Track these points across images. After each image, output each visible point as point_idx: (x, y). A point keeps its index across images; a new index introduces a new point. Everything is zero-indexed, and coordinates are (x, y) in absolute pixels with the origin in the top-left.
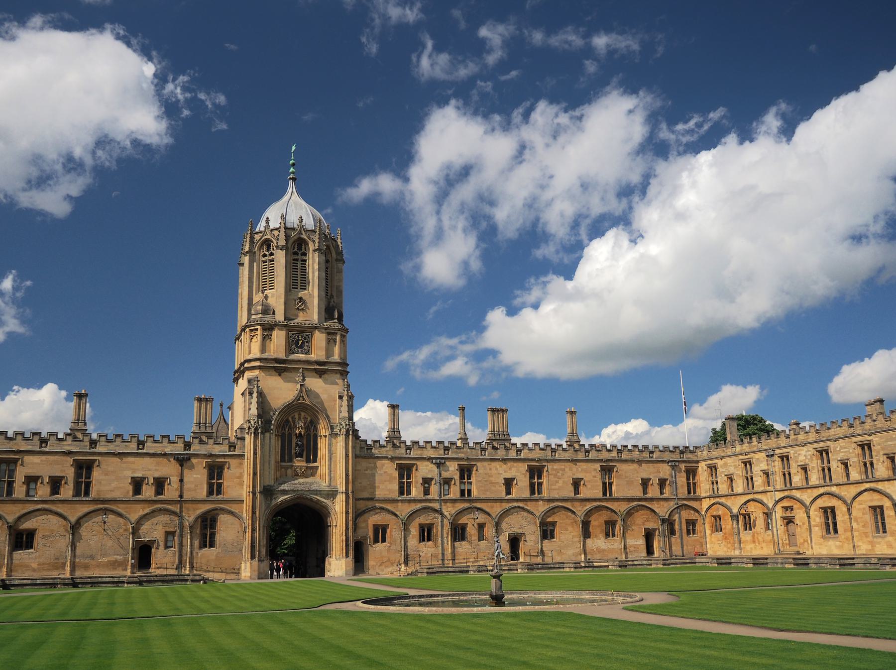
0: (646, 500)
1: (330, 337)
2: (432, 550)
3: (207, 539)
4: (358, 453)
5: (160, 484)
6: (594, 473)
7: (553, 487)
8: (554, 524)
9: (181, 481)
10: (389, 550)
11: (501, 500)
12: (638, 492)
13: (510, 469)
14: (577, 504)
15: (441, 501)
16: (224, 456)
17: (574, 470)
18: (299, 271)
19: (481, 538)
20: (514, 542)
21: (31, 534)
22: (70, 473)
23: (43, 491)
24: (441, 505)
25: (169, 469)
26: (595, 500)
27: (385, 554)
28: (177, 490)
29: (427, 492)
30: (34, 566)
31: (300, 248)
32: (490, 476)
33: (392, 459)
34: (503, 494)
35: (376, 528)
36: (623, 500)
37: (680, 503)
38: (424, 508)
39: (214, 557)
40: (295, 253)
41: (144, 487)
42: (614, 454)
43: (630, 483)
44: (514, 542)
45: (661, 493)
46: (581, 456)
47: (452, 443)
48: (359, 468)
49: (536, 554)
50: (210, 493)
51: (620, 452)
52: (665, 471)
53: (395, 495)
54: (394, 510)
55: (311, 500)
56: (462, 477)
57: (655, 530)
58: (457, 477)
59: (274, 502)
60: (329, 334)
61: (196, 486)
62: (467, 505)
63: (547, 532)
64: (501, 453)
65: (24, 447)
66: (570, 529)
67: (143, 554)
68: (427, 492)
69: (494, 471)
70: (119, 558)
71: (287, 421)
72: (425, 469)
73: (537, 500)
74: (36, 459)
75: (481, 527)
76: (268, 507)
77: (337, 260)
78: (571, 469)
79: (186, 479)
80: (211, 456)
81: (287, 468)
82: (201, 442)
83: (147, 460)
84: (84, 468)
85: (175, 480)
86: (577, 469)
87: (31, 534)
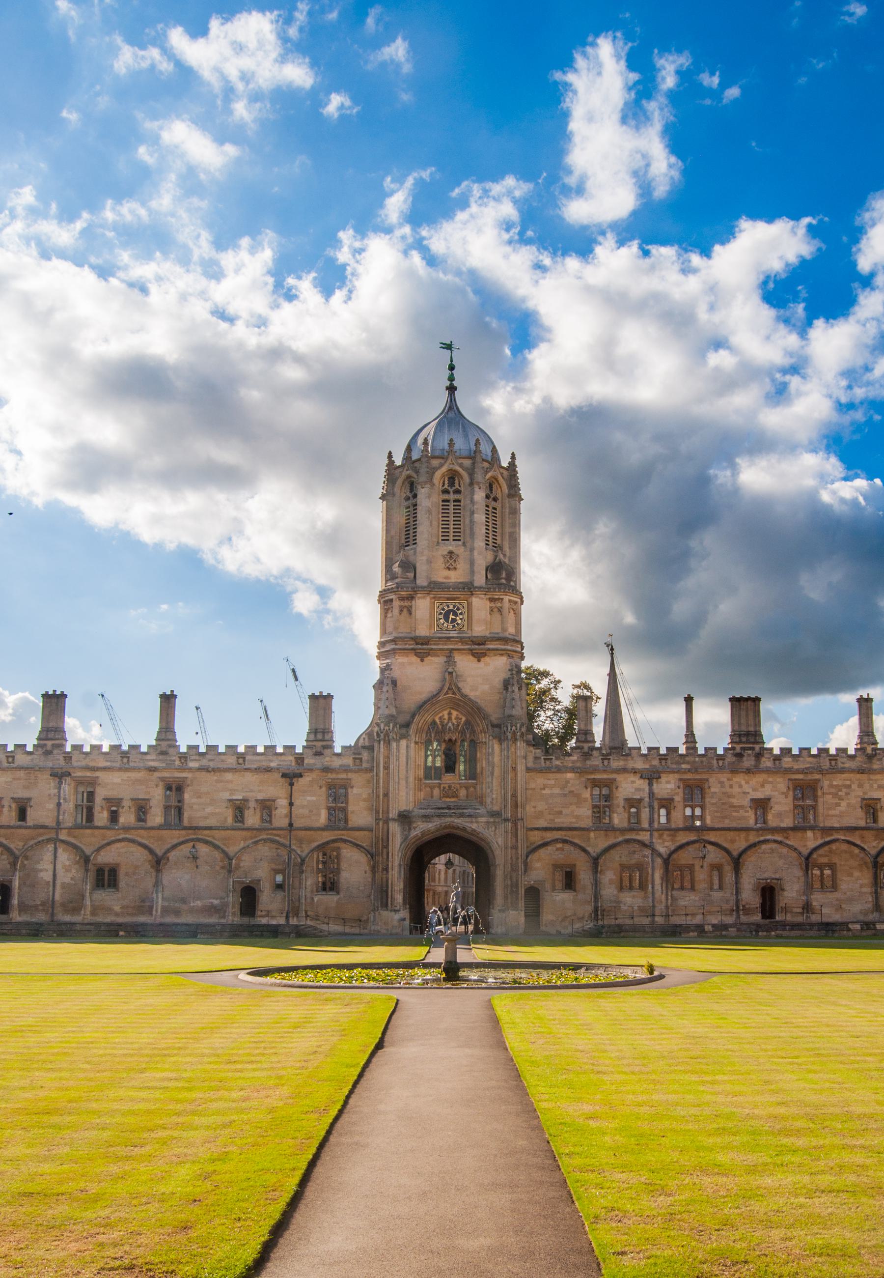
1: (493, 605)
4: (530, 765)
7: (832, 812)
9: (291, 804)
11: (747, 830)
13: (763, 786)
14: (869, 835)
17: (867, 786)
18: (451, 515)
20: (768, 894)
22: (157, 796)
24: (651, 835)
25: (276, 790)
28: (286, 816)
30: (117, 908)
32: (729, 797)
38: (627, 841)
39: (334, 905)
40: (446, 492)
41: (247, 813)
44: (768, 894)
47: (672, 750)
48: (532, 785)
49: (800, 910)
53: (587, 822)
54: (583, 845)
55: (464, 829)
59: (413, 833)
60: (492, 600)
61: (311, 811)
62: (692, 837)
64: (748, 762)
65: (102, 764)
66: (857, 874)
67: (249, 896)
69: (736, 790)
70: (216, 902)
71: (434, 722)
72: (630, 787)
73: (804, 829)
76: (405, 839)
77: (510, 496)
78: (860, 786)
79: (297, 802)
80: (326, 770)
81: (432, 788)
82: (318, 754)
84: (176, 788)
85: (283, 802)
86: (871, 786)
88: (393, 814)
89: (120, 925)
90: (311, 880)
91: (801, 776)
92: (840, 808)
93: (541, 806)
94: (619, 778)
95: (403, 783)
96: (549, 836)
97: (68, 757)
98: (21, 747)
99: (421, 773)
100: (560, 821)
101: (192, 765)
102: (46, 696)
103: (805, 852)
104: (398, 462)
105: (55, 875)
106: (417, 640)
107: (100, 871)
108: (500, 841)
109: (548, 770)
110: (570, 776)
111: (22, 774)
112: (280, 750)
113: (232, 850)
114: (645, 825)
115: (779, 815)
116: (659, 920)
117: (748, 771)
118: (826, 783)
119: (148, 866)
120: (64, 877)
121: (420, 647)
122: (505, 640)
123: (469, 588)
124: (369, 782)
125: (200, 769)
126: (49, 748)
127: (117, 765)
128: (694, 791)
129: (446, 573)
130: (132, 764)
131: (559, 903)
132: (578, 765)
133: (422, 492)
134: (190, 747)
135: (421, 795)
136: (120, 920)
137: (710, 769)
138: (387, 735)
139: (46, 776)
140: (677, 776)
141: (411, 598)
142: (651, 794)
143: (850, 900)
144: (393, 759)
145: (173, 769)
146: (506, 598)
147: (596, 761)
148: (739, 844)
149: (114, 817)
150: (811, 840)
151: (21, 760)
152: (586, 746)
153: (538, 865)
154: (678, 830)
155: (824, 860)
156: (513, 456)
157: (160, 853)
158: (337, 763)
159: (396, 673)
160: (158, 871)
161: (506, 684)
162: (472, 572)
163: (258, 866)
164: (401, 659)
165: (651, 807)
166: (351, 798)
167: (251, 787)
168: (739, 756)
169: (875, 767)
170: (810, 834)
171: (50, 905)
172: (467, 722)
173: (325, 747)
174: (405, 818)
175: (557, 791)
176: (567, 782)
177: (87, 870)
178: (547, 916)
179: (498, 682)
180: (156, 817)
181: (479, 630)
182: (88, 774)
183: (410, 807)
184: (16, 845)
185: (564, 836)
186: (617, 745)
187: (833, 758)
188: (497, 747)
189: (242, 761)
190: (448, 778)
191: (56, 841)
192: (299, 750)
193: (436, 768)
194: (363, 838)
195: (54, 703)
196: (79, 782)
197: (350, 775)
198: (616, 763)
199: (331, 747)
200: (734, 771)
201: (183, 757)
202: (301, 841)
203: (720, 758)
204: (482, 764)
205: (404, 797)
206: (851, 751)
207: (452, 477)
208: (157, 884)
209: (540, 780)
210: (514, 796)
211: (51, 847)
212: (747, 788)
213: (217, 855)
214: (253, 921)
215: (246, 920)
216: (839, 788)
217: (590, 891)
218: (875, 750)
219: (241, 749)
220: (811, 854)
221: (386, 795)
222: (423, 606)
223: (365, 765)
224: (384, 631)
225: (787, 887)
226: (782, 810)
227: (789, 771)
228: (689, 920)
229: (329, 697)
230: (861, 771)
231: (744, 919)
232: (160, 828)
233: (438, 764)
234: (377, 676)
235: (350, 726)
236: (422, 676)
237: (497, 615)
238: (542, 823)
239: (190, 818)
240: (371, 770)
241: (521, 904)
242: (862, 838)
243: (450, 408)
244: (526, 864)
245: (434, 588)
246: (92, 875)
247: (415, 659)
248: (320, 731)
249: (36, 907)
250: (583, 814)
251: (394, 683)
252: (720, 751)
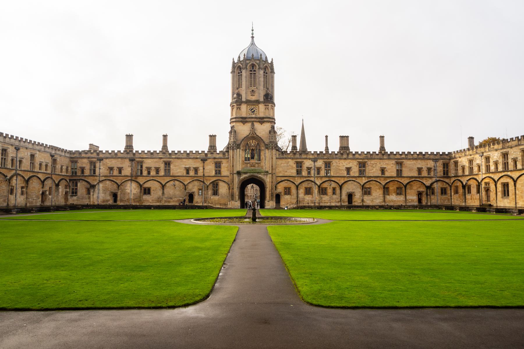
0: (419, 177)
2: (310, 199)
3: (215, 193)
4: (277, 157)
5: (196, 170)
6: (392, 165)
8: (370, 188)
9: (204, 169)
10: (291, 198)
11: (344, 177)
12: (416, 174)
14: (382, 179)
15: (314, 177)
16: (221, 158)
17: (382, 163)
19: (334, 193)
20: (350, 196)
21: (149, 189)
22: (162, 166)
23: (153, 173)
25: (198, 164)
26: (392, 177)
27: (289, 199)
29: (309, 173)
30: (151, 201)
31: (253, 68)
33: (292, 159)
34: (345, 175)
35: (285, 188)
36: (407, 177)
37: (438, 179)
38: (307, 180)
41: (190, 171)
42: (403, 156)
43: (411, 170)
44: (350, 196)
45: (429, 174)
46: (385, 157)
47: (321, 152)
48: (278, 163)
50: (216, 173)
51: (406, 155)
52: (431, 164)
56: (326, 167)
57: (423, 192)
58: (323, 167)
59: (241, 178)
60: (265, 105)
62: (327, 179)
63: (366, 191)
64: (345, 156)
66: (378, 191)
68: (309, 173)
69: (341, 164)
71: (248, 144)
72: (308, 163)
73: (362, 177)
74: (149, 161)
75: (334, 189)
76: (239, 179)
77: (271, 72)
78: (380, 163)
79: (205, 168)
80: (215, 158)
81: (247, 163)
82: (212, 153)
83: (191, 160)
84: (168, 164)
87: (149, 189)
88: (235, 172)
89: (152, 206)
90: (210, 192)
91: (361, 161)
92: (373, 169)
93: (281, 169)
94: (305, 161)
95: (238, 162)
96: (283, 179)
97: (134, 154)
98: (119, 151)
99: (244, 159)
100: (286, 174)
101: (173, 157)
102: (127, 135)
103: (362, 184)
104: (236, 62)
105: (131, 191)
106: (242, 118)
107: (145, 189)
108: (268, 180)
109: (283, 158)
110: (289, 160)
111: (120, 160)
112: (200, 152)
113: (186, 183)
114: (313, 175)
115: (354, 172)
116: (317, 204)
117: (345, 159)
118: (369, 163)
119: (160, 188)
120: (134, 191)
121: (243, 120)
122: (269, 118)
123: (257, 102)
124: (228, 162)
125: (175, 158)
126: (128, 151)
127: (149, 157)
128: (328, 165)
129: (251, 97)
130: (154, 157)
131: (285, 200)
132: (292, 157)
133: (244, 72)
134: (172, 151)
135: (244, 166)
136: (151, 204)
137: (333, 159)
138: (233, 147)
139: (128, 160)
140: (323, 160)
141: (240, 105)
142: (315, 166)
143: (376, 199)
144: (235, 155)
145: (167, 157)
146: (270, 105)
147: (297, 156)
148: (341, 181)
149: (149, 173)
150: (364, 180)
151: (119, 155)
152: (295, 151)
153: (280, 187)
154: (322, 177)
155: (368, 186)
156: (272, 60)
157: (164, 184)
158: (218, 156)
159: (235, 129)
160: (163, 189)
161: (270, 132)
162: (260, 97)
163: (194, 188)
164: (238, 124)
165: (315, 170)
166: (222, 167)
167: (191, 164)
168: (342, 154)
169: (385, 158)
170: (364, 178)
171: (128, 200)
172: (258, 144)
173: (215, 151)
174: (239, 173)
175: (285, 165)
176: (289, 162)
177: (141, 189)
178: (283, 203)
179: (267, 131)
180: (162, 173)
181: (261, 115)
182: (141, 160)
183: (240, 170)
184: (119, 182)
185: (288, 179)
186: (304, 151)
187: (372, 155)
188: (267, 151)
189: (188, 155)
190: (252, 161)
191: (131, 180)
192: (206, 152)
193: (249, 158)
194: (226, 179)
195: (129, 137)
196: (138, 162)
197: (222, 160)
198: (304, 156)
199: (216, 151)
200: (340, 159)
201: (170, 154)
202: (207, 180)
203: (336, 154)
204: (262, 156)
205: (239, 167)
206: (377, 153)
207: (253, 66)
208: (163, 193)
209: (280, 162)
210: (272, 166)
211: (129, 182)
212: (344, 164)
213: (181, 184)
214: (192, 204)
215: (190, 204)
216: (373, 164)
217: (295, 195)
218: (385, 152)
219: (188, 152)
220: (364, 185)
221: (233, 166)
222: (244, 107)
223: (226, 157)
224: (232, 115)
225: (356, 194)
226: (355, 171)
227: (358, 159)
228: (326, 204)
229: (215, 136)
230: (381, 159)
231: (343, 204)
232: (163, 176)
233: (249, 156)
234: (230, 129)
235: (221, 145)
236: (244, 130)
237: (267, 110)
238: (281, 175)
239: (173, 173)
240: (228, 158)
241: (274, 199)
242: (380, 180)
243: (252, 44)
244: (276, 187)
245: (248, 102)
246: (143, 191)
247: (242, 124)
248: (213, 147)
249: (125, 201)
250: (293, 172)
251: (235, 132)
252: (336, 153)
